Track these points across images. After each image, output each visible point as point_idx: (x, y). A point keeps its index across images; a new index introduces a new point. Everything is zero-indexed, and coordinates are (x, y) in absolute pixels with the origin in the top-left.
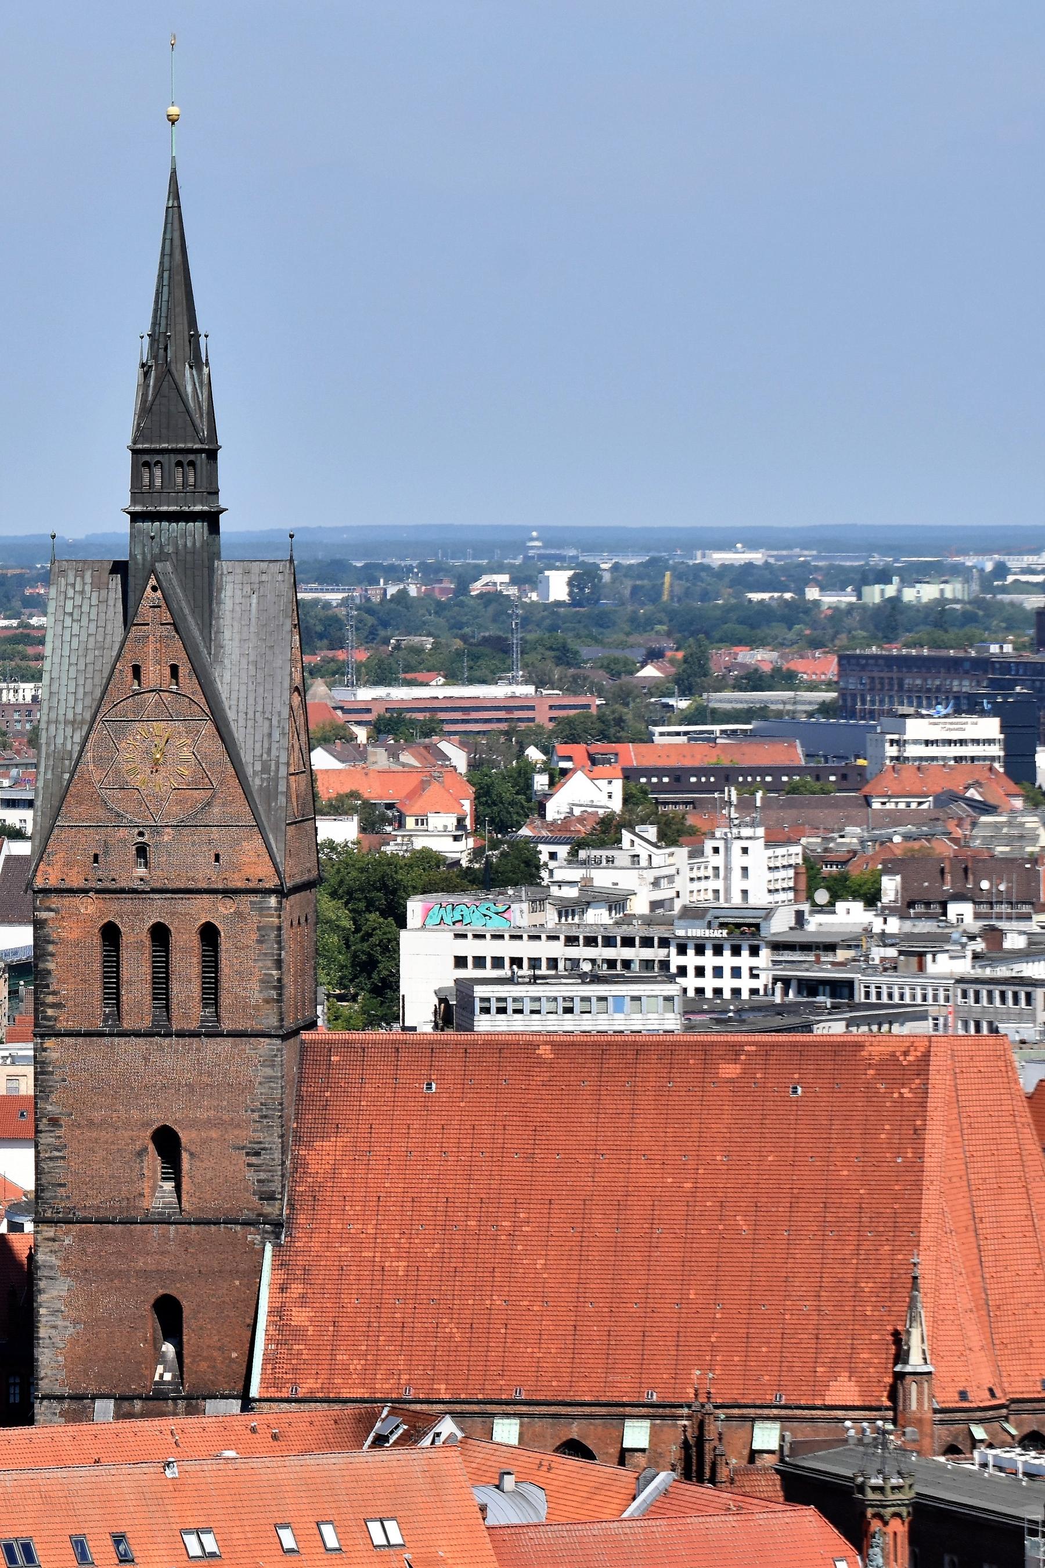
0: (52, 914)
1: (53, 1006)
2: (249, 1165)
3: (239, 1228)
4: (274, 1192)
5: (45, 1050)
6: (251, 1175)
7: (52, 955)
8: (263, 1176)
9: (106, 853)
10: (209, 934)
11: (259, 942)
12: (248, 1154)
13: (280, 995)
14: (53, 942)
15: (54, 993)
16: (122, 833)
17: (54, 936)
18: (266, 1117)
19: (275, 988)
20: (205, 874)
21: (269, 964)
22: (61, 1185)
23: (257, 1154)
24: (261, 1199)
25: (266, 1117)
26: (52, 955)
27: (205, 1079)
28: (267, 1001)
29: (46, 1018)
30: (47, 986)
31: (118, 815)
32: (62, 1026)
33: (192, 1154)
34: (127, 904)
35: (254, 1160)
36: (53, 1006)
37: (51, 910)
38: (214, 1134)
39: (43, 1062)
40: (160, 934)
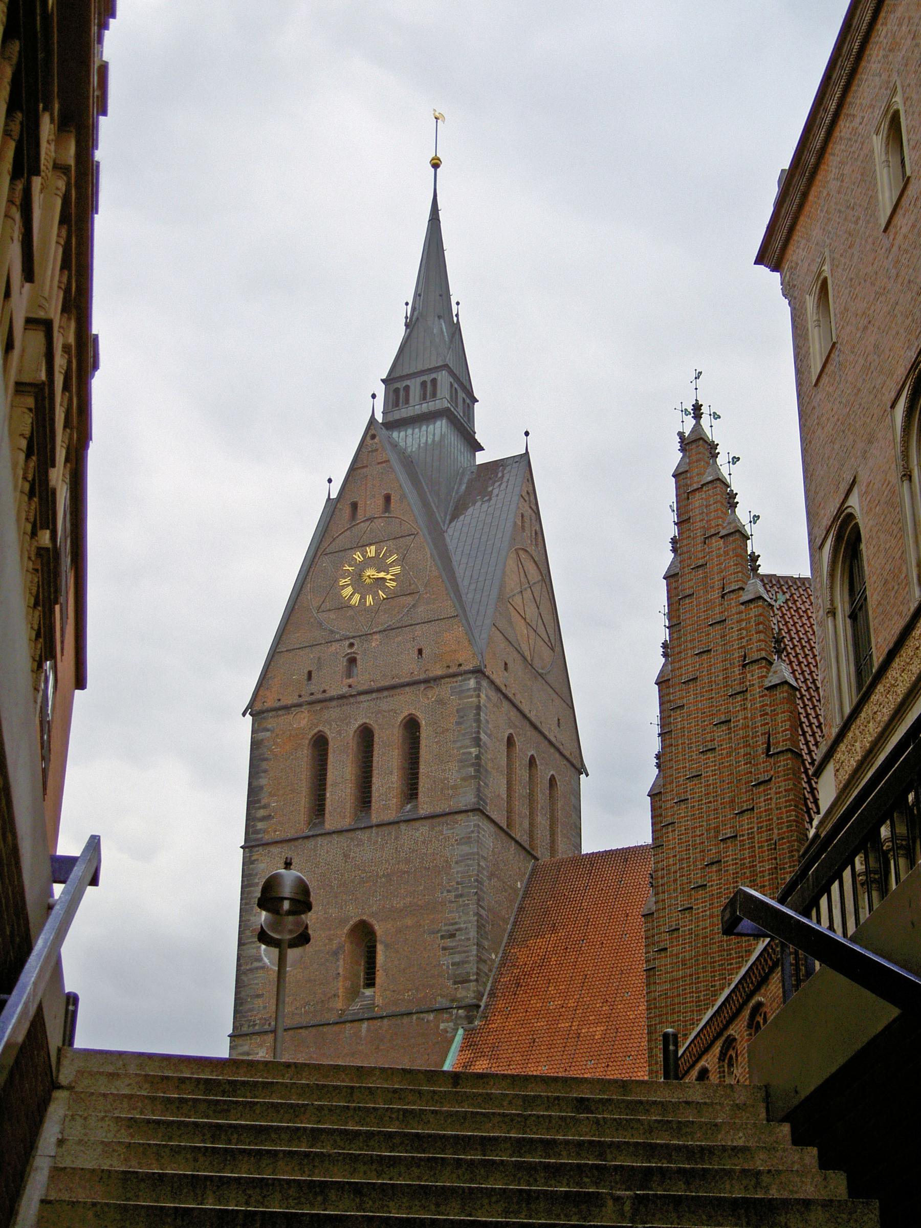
0: (268, 734)
1: (263, 819)
2: (444, 949)
3: (431, 1017)
4: (468, 973)
5: (252, 862)
6: (446, 960)
7: (265, 771)
8: (457, 958)
9: (319, 668)
10: (412, 726)
11: (458, 723)
12: (442, 937)
13: (477, 771)
14: (266, 759)
15: (265, 807)
16: (334, 647)
17: (268, 754)
18: (461, 896)
19: (473, 765)
20: (409, 667)
21: (468, 742)
22: (259, 996)
23: (452, 936)
24: (455, 983)
25: (461, 896)
26: (265, 771)
27: (403, 867)
28: (464, 779)
29: (256, 832)
30: (259, 801)
31: (332, 632)
32: (267, 838)
33: (387, 946)
34: (334, 712)
35: (449, 943)
36: (263, 819)
37: (268, 730)
38: (409, 921)
39: (250, 875)
40: (366, 736)
